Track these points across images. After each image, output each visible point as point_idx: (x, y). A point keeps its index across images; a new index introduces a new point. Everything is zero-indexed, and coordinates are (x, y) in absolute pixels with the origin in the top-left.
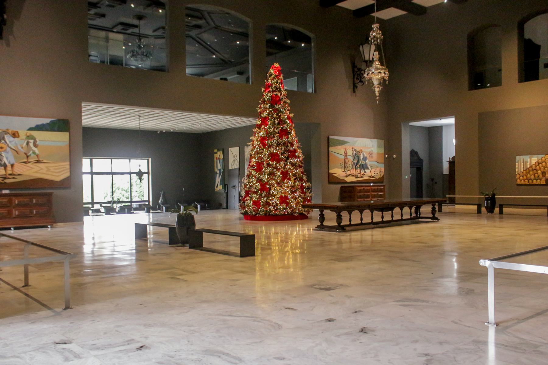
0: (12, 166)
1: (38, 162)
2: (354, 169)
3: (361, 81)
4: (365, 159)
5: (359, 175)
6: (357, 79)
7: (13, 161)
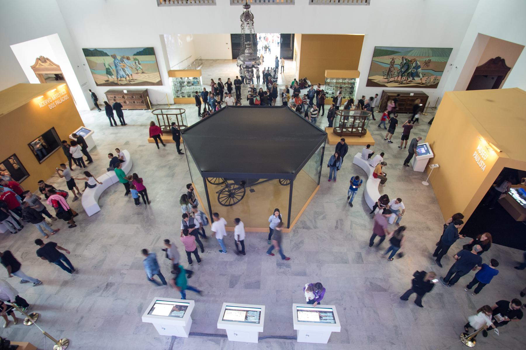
0: (131, 75)
1: (143, 73)
2: (400, 77)
4: (417, 67)
5: (405, 82)
7: (131, 73)
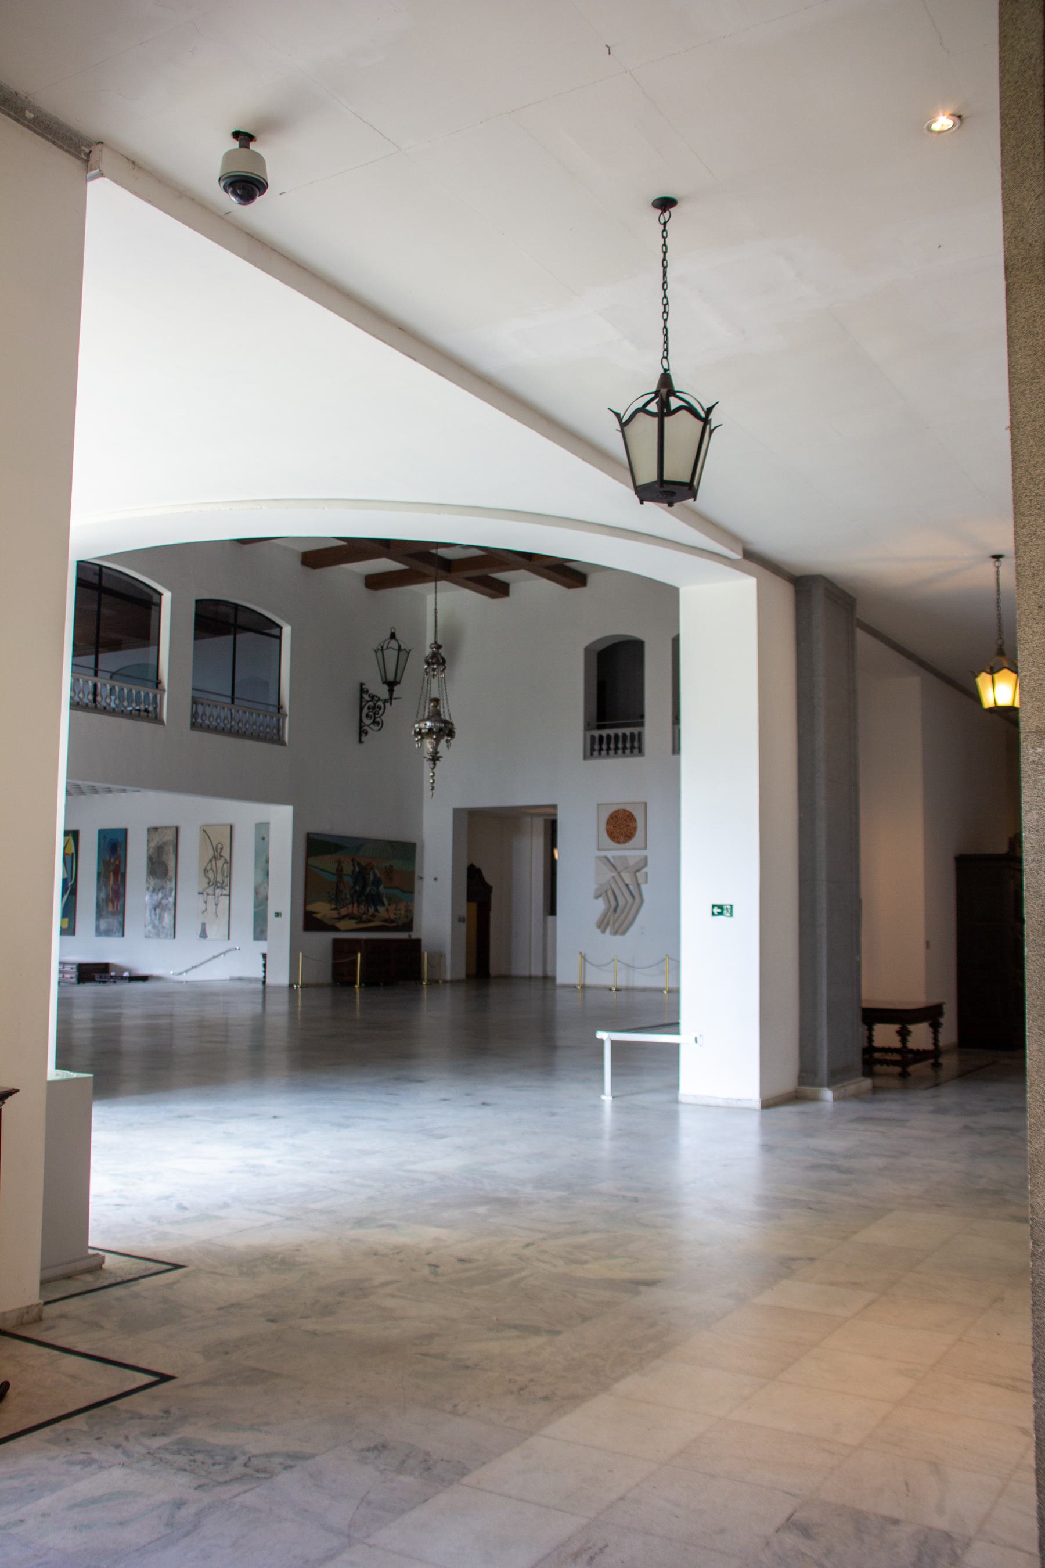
2: (356, 905)
3: (374, 722)
6: (367, 716)
